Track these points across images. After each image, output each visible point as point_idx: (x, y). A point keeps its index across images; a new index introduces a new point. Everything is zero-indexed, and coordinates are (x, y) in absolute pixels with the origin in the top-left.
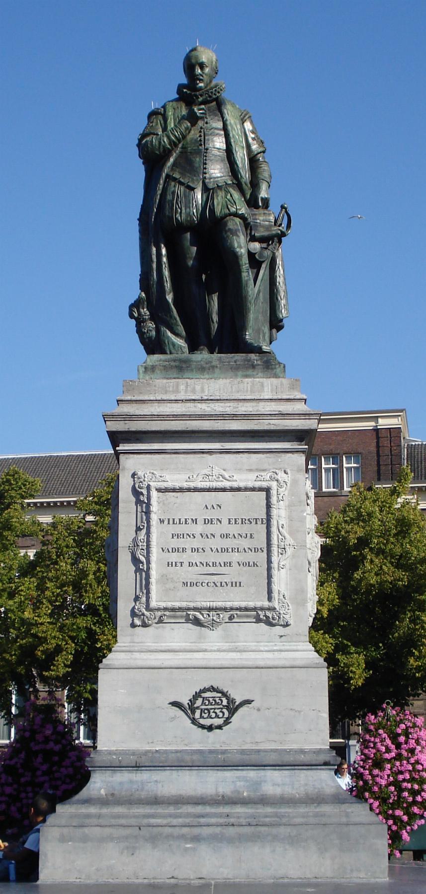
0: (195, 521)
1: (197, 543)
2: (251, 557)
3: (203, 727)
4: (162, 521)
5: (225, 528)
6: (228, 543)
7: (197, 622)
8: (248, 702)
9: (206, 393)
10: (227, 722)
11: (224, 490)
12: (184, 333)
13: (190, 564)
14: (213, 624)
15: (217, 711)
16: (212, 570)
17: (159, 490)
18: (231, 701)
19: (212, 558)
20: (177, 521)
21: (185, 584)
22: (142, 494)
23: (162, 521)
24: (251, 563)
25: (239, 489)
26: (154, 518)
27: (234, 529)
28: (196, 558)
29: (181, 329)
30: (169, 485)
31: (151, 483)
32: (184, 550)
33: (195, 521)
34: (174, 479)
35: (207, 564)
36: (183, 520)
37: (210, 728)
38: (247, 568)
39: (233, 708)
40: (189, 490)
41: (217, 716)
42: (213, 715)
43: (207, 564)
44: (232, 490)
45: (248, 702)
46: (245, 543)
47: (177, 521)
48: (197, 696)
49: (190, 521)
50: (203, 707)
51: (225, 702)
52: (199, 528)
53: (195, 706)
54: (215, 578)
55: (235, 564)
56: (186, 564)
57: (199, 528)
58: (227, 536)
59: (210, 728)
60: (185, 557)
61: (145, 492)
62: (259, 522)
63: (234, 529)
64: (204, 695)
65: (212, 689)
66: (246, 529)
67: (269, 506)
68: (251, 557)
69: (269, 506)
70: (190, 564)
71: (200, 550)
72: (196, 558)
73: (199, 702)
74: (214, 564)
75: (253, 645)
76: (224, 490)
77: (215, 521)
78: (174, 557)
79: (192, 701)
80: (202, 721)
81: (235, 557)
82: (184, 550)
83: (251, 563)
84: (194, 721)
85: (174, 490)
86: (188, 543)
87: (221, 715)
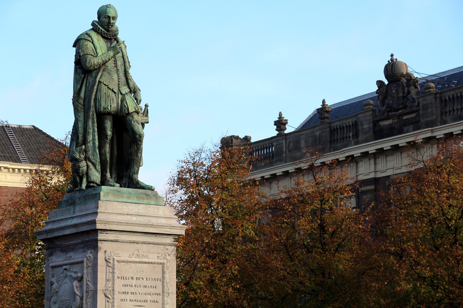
0: (132, 278)
1: (133, 290)
2: (155, 298)
4: (118, 278)
5: (145, 282)
9: (135, 211)
11: (145, 263)
12: (100, 170)
13: (130, 300)
16: (139, 304)
17: (118, 261)
19: (139, 297)
20: (125, 278)
22: (110, 263)
23: (118, 278)
25: (152, 263)
26: (116, 275)
27: (148, 283)
28: (133, 297)
29: (99, 167)
30: (122, 259)
31: (115, 257)
32: (128, 293)
33: (132, 278)
34: (124, 257)
35: (138, 301)
38: (154, 303)
40: (131, 262)
44: (149, 263)
46: (152, 291)
47: (125, 278)
49: (130, 278)
52: (134, 282)
56: (129, 300)
58: (145, 287)
60: (128, 297)
61: (111, 261)
62: (159, 280)
63: (148, 283)
66: (153, 283)
67: (163, 273)
68: (155, 298)
69: (163, 273)
70: (130, 300)
72: (133, 297)
74: (140, 301)
76: (145, 263)
77: (141, 279)
78: (123, 297)
81: (149, 298)
82: (128, 293)
85: (124, 262)
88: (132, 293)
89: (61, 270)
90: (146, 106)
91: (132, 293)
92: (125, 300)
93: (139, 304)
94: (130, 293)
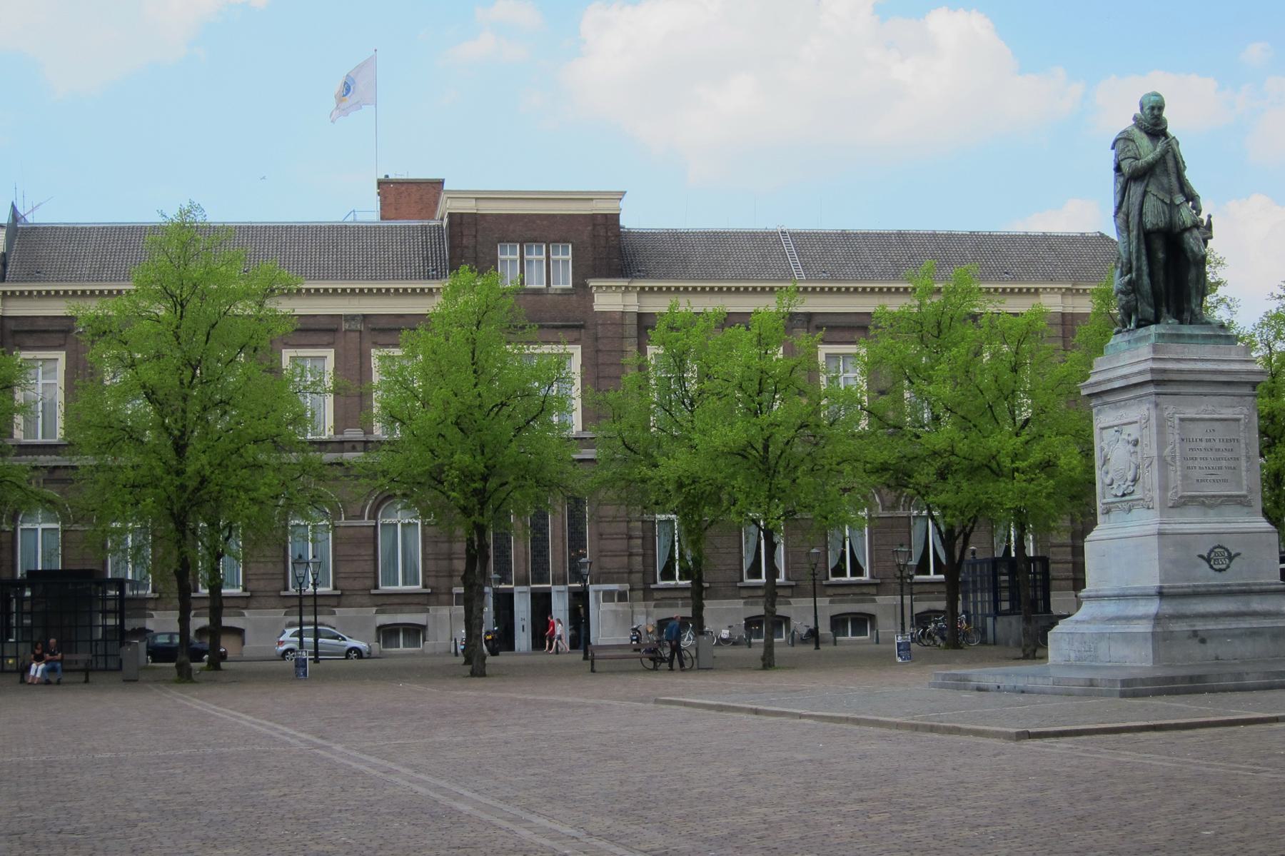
1: (1202, 455)
6: (1219, 455)
7: (1203, 504)
8: (1238, 554)
14: (1211, 506)
18: (1230, 554)
28: (1203, 464)
37: (1220, 570)
39: (1231, 558)
48: (1212, 551)
52: (1203, 445)
57: (1203, 445)
59: (1220, 570)
60: (1196, 464)
63: (1222, 446)
65: (1219, 547)
66: (1229, 446)
72: (1203, 464)
75: (1233, 519)
78: (1190, 463)
81: (1224, 463)
84: (1211, 567)
89: (1112, 431)
90: (1210, 217)
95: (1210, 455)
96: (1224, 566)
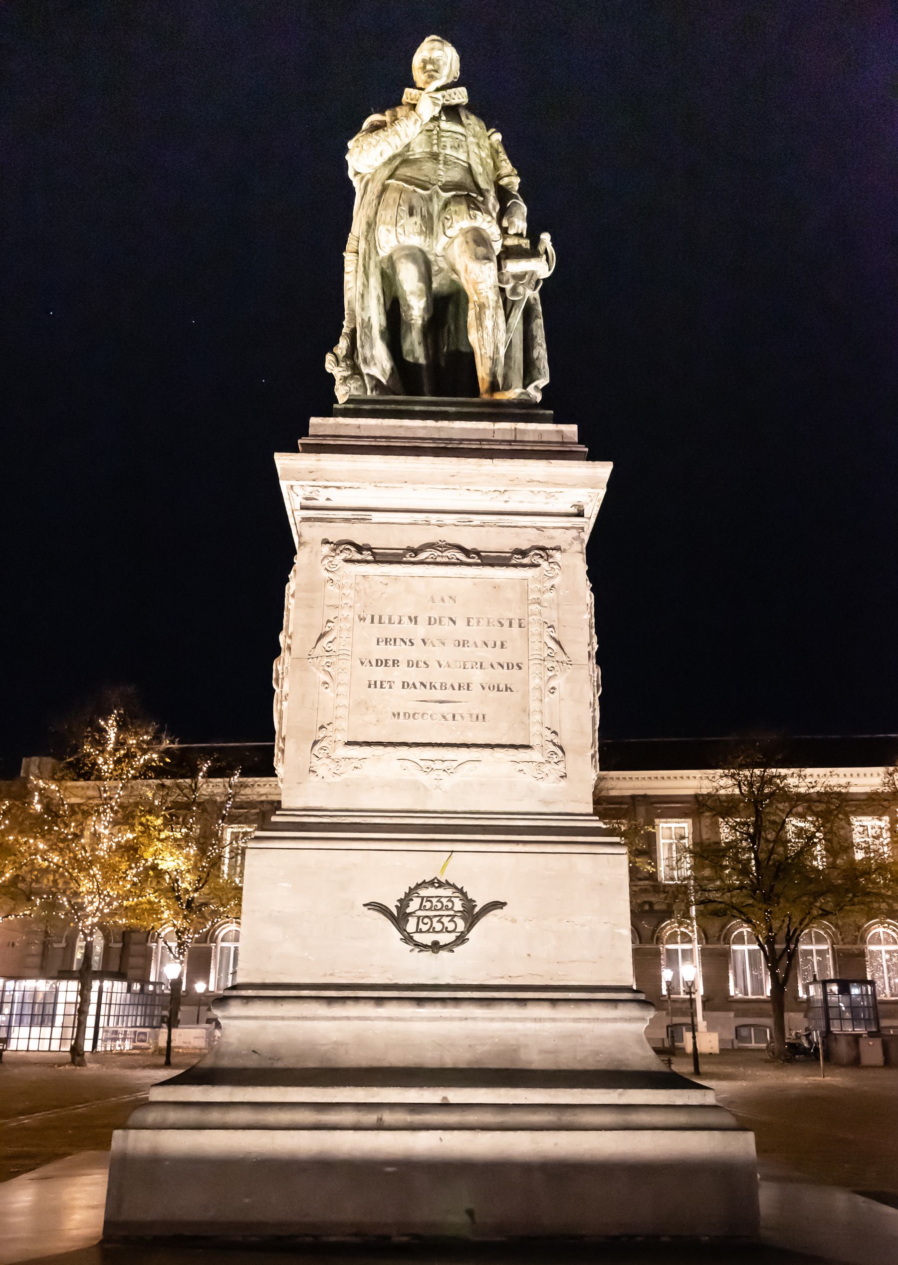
0: (414, 620)
1: (414, 653)
2: (502, 676)
3: (422, 947)
5: (461, 630)
8: (498, 905)
10: (461, 939)
15: (445, 920)
16: (439, 694)
18: (469, 904)
19: (436, 675)
21: (396, 715)
24: (502, 687)
32: (395, 663)
33: (414, 620)
35: (433, 686)
36: (395, 619)
39: (472, 915)
41: (446, 930)
42: (438, 927)
43: (433, 686)
45: (498, 905)
47: (385, 619)
48: (411, 893)
49: (405, 620)
50: (419, 913)
51: (458, 905)
52: (421, 631)
53: (408, 911)
54: (444, 708)
55: (475, 687)
60: (397, 675)
64: (423, 892)
68: (502, 676)
71: (421, 664)
72: (415, 675)
73: (414, 905)
74: (443, 686)
78: (379, 674)
79: (404, 902)
80: (417, 937)
82: (395, 663)
83: (502, 687)
84: (408, 939)
86: (401, 652)
87: (451, 926)
88: (410, 664)
91: (410, 664)
92: (385, 685)
93: (439, 694)
94: (403, 665)
95: (448, 653)
96: (445, 939)
